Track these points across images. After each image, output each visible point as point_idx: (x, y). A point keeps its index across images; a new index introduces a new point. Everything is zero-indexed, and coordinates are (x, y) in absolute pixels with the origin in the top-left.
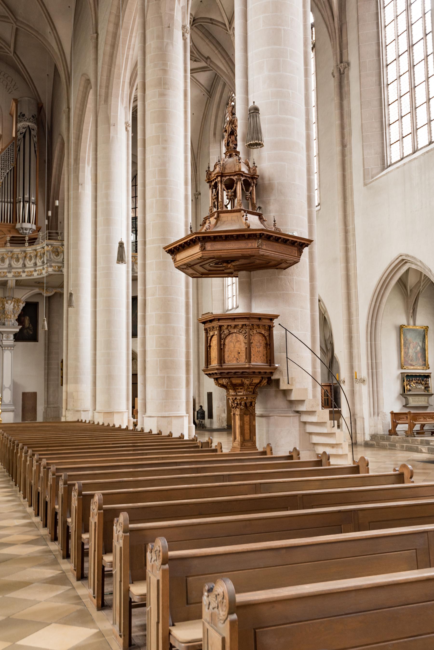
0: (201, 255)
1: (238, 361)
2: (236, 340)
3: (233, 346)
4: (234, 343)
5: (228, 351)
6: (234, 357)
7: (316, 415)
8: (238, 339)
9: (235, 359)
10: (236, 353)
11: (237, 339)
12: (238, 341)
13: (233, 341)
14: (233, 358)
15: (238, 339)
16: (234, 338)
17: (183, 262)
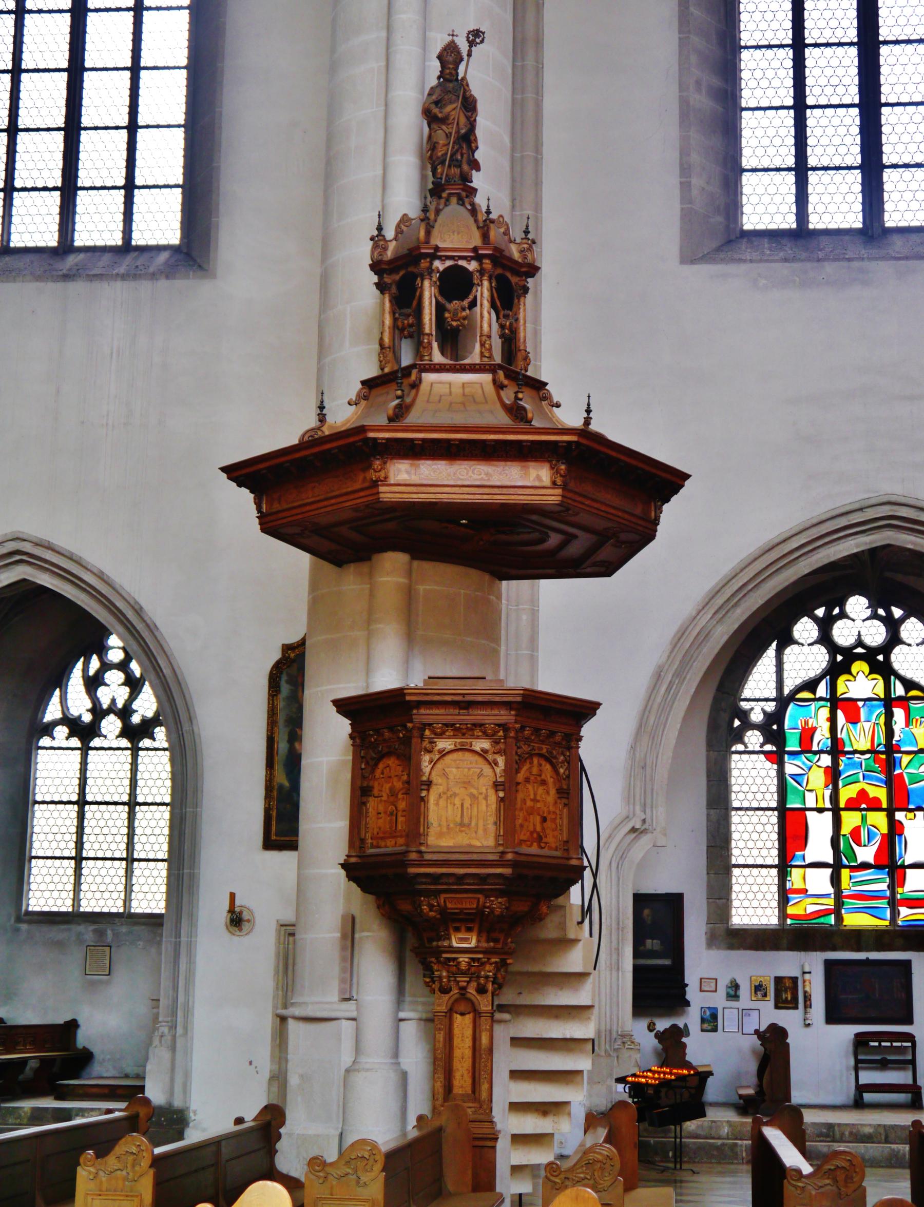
0: (559, 498)
1: (543, 845)
2: (539, 779)
3: (532, 797)
4: (534, 787)
5: (521, 809)
6: (535, 829)
7: (589, 1018)
8: (543, 777)
9: (535, 835)
10: (538, 818)
11: (540, 776)
12: (544, 783)
13: (532, 778)
14: (532, 833)
15: (543, 777)
16: (535, 770)
17: (440, 496)
